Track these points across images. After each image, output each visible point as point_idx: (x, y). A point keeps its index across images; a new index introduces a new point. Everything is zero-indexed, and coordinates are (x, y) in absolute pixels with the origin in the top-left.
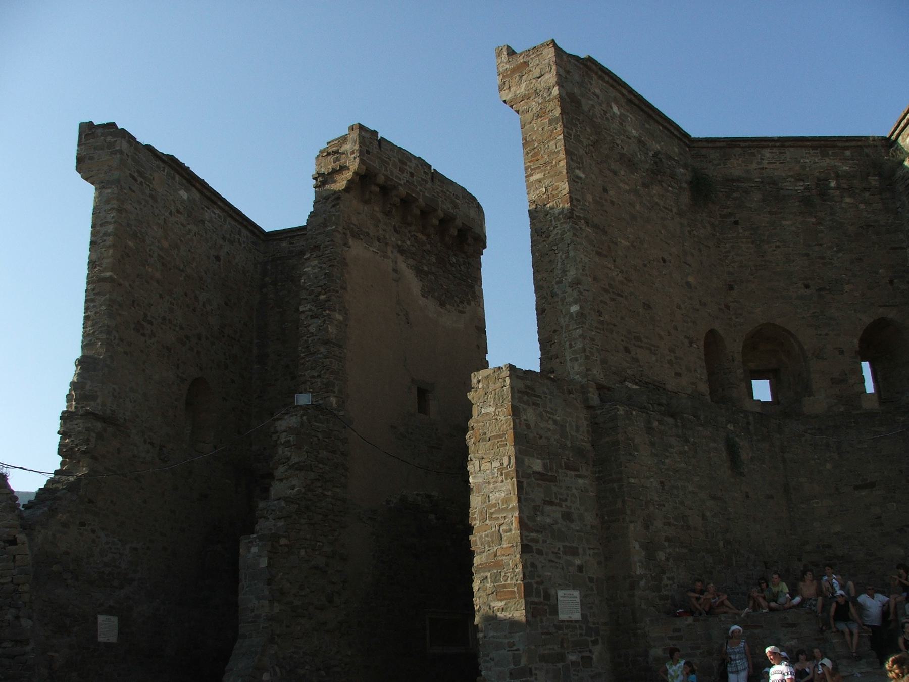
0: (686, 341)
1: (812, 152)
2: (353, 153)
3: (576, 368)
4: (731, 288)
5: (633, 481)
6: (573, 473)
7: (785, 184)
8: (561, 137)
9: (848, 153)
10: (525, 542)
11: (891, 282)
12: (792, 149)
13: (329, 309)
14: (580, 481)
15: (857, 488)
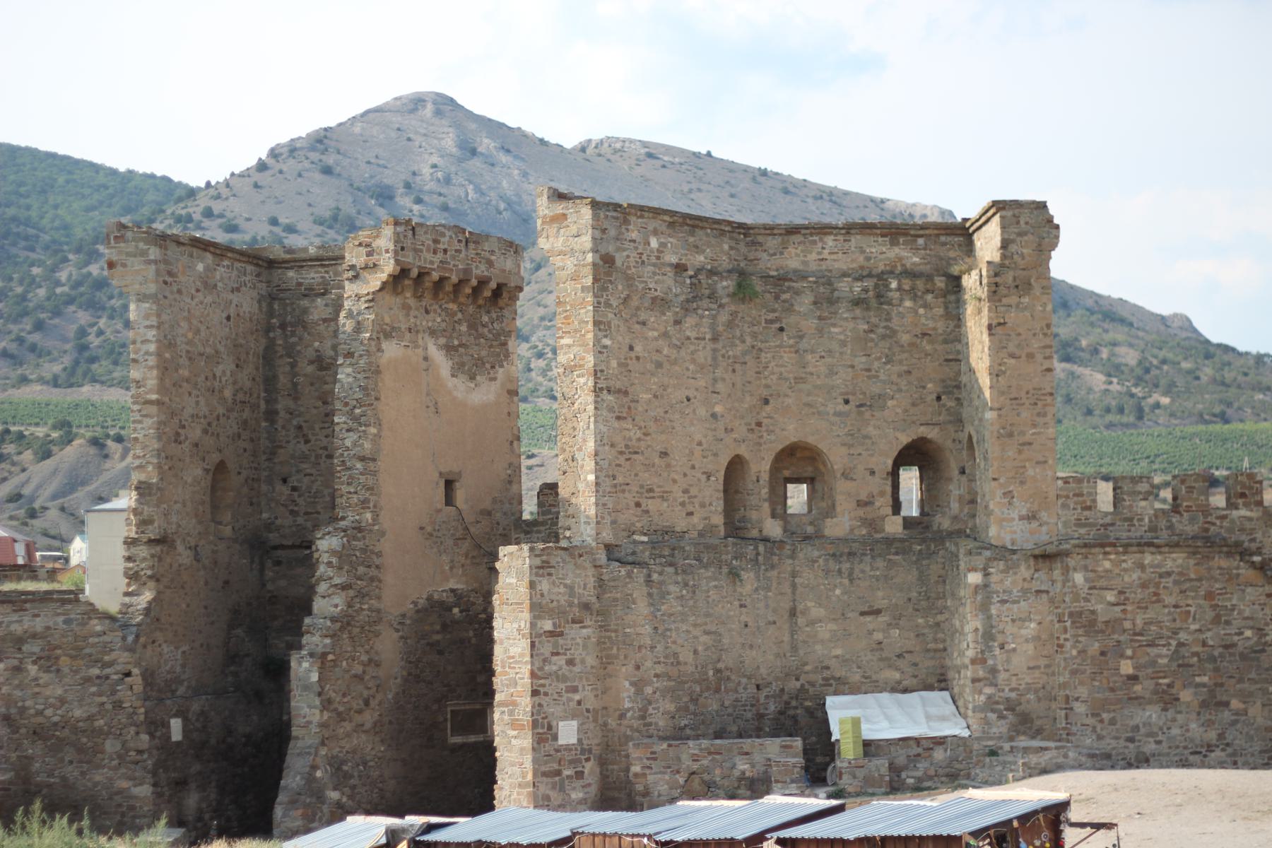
0: (704, 477)
1: (880, 239)
2: (387, 251)
3: (588, 531)
4: (766, 402)
5: (628, 630)
6: (578, 625)
7: (841, 284)
8: (591, 308)
9: (921, 241)
10: (535, 688)
11: (939, 398)
12: (858, 237)
13: (365, 425)
14: (584, 631)
15: (863, 614)
